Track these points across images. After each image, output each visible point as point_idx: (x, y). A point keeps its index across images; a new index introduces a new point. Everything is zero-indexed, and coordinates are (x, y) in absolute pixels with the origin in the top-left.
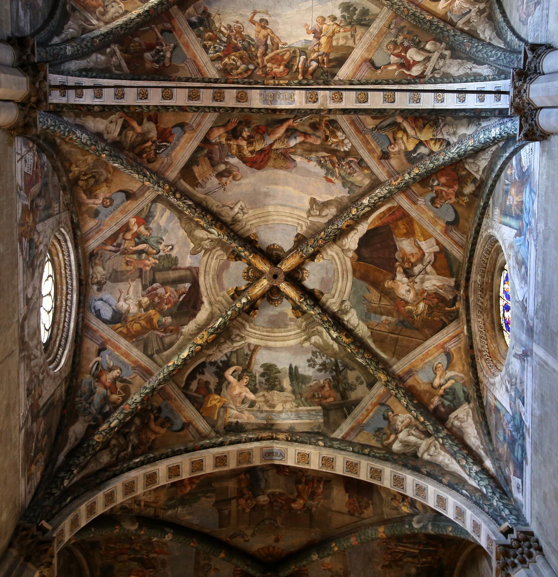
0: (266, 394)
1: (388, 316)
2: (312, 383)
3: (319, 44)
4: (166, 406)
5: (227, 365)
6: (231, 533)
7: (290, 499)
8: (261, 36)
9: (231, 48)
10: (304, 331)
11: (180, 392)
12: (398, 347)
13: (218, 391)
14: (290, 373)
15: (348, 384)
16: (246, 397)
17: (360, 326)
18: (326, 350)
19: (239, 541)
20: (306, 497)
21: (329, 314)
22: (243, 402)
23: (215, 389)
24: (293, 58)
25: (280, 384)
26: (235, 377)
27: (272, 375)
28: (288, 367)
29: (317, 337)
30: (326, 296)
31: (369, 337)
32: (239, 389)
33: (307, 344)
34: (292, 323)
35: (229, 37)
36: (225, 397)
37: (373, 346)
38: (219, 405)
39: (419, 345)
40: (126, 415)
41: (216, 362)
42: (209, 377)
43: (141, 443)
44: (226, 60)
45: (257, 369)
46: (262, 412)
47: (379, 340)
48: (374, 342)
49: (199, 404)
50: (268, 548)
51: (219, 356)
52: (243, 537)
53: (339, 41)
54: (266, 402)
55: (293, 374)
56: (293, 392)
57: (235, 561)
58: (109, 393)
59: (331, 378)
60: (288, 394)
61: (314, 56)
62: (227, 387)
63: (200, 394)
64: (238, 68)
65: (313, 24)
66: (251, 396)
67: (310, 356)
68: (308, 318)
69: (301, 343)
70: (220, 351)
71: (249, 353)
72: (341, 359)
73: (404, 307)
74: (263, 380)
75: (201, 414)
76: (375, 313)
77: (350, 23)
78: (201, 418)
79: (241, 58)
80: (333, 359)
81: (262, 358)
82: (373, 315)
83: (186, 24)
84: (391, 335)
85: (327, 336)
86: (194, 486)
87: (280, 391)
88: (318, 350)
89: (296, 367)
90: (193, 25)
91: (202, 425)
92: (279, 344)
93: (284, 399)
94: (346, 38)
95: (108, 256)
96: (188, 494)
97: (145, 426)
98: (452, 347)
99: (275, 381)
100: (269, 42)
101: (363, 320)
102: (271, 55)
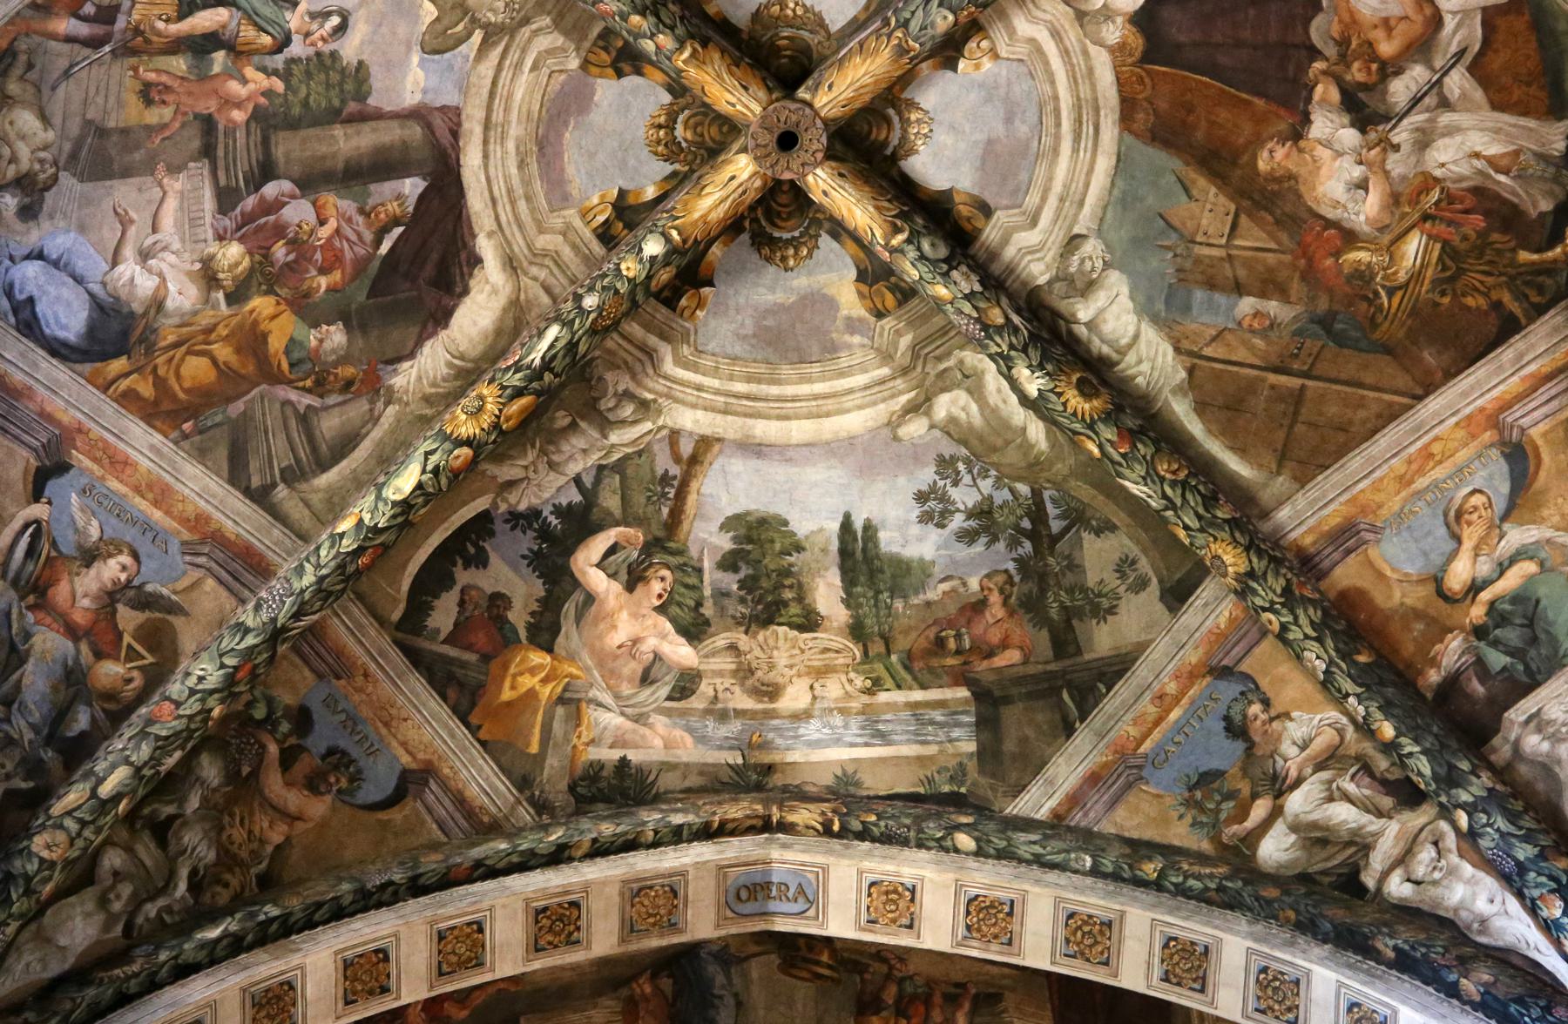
0: (743, 641)
1: (1263, 295)
5: (581, 521)
10: (905, 371)
12: (1300, 429)
13: (544, 633)
14: (845, 553)
16: (657, 657)
17: (1142, 344)
18: (995, 450)
21: (1010, 297)
22: (646, 679)
23: (531, 628)
25: (800, 599)
26: (613, 576)
27: (770, 563)
28: (834, 526)
29: (961, 396)
30: (1001, 218)
31: (1179, 390)
32: (629, 620)
33: (916, 428)
34: (856, 339)
36: (572, 658)
37: (1195, 427)
38: (546, 692)
39: (1391, 415)
40: (164, 745)
41: (535, 513)
42: (508, 577)
43: (228, 859)
46: (723, 716)
47: (1223, 399)
48: (1201, 408)
49: (464, 693)
51: (547, 487)
54: (744, 673)
55: (858, 555)
56: (857, 631)
60: (832, 638)
62: (579, 619)
66: (681, 652)
67: (927, 475)
68: (925, 318)
69: (893, 424)
70: (552, 466)
71: (675, 470)
72: (1057, 486)
73: (1337, 254)
74: (731, 582)
75: (474, 730)
76: (1211, 285)
78: (476, 751)
80: (1023, 489)
81: (725, 493)
82: (1199, 295)
84: (1273, 378)
85: (1002, 393)
87: (802, 628)
88: (964, 451)
89: (869, 527)
91: (481, 780)
92: (799, 430)
95: (63, 63)
97: (243, 786)
98: (1535, 422)
99: (779, 586)
101: (1155, 320)
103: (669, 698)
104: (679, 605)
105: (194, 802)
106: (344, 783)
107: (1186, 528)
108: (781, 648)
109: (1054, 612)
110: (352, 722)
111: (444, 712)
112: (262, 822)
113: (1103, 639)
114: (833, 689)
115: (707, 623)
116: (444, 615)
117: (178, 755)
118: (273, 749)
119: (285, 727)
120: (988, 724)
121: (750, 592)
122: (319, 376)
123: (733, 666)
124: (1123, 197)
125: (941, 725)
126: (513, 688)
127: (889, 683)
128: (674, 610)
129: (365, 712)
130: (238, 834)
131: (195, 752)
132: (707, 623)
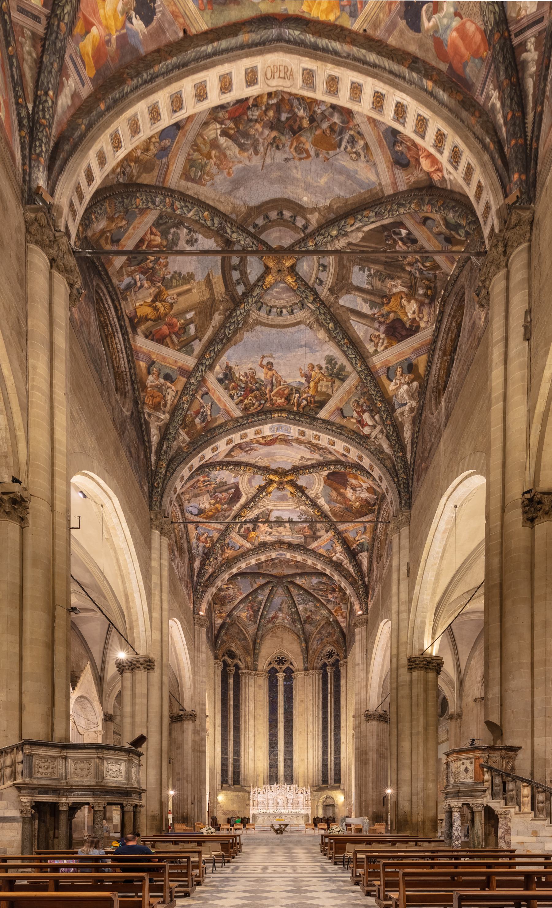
3: (309, 387)
8: (268, 377)
9: (248, 391)
24: (291, 394)
35: (246, 383)
44: (246, 401)
53: (323, 387)
61: (305, 396)
64: (254, 404)
65: (305, 369)
77: (331, 375)
79: (255, 397)
83: (216, 382)
90: (220, 381)
94: (327, 386)
100: (274, 381)
102: (275, 390)
108: (281, 529)
113: (318, 534)
116: (242, 530)
122: (225, 510)
124: (324, 490)
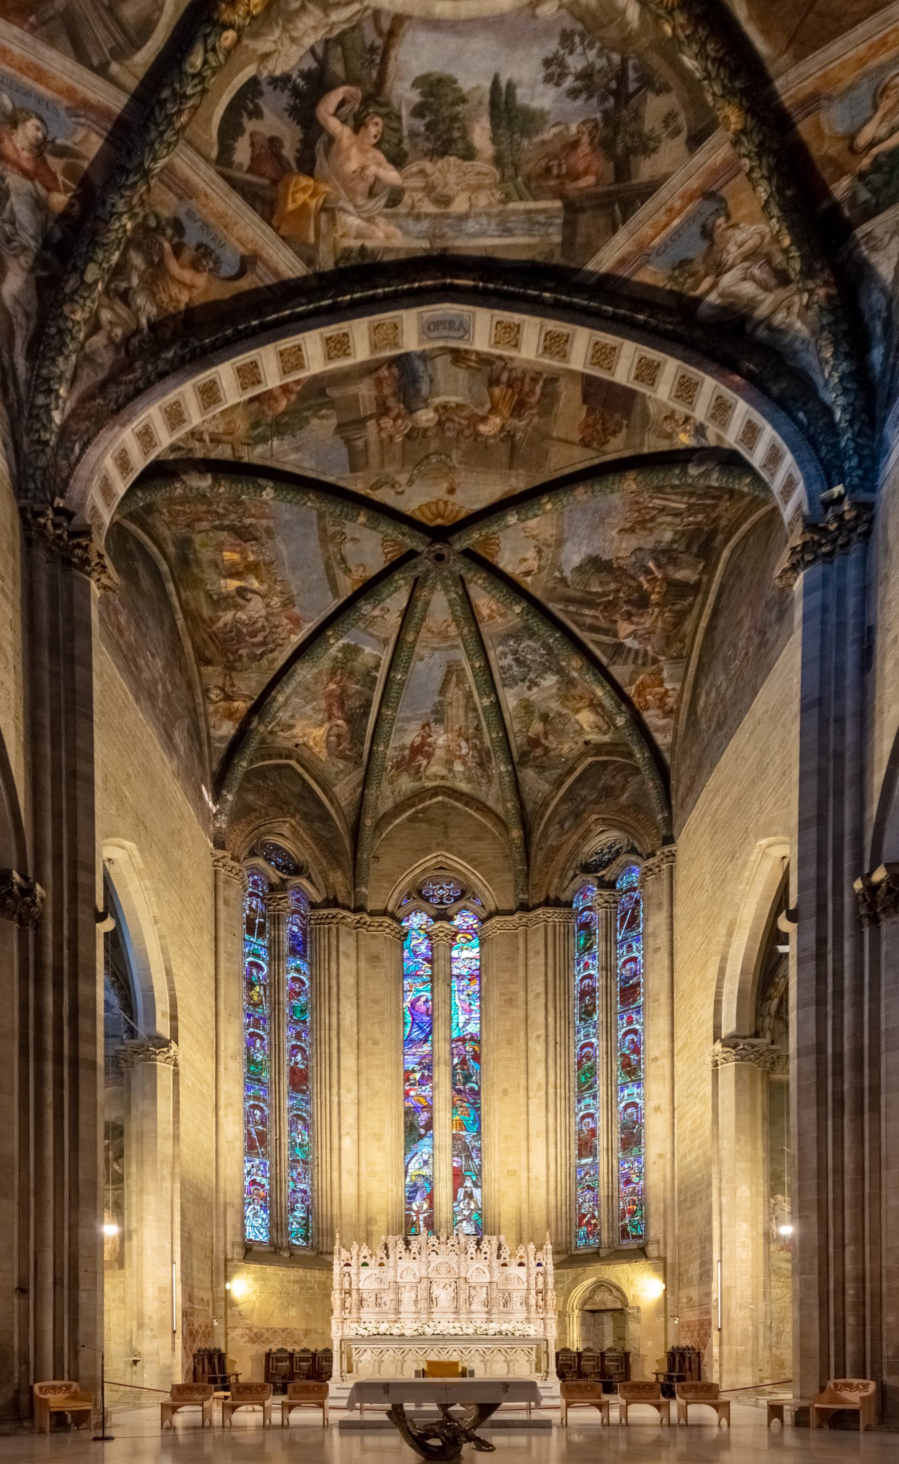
0: (429, 167)
2: (548, 134)
4: (190, 214)
6: (373, 481)
7: (476, 415)
11: (211, 173)
15: (641, 135)
16: (377, 179)
19: (384, 496)
20: (506, 412)
38: (313, 203)
45: (404, 93)
46: (418, 217)
50: (437, 503)
52: (393, 487)
54: (429, 189)
57: (383, 528)
58: (42, 192)
59: (598, 116)
60: (483, 165)
62: (327, 152)
63: (262, 175)
66: (391, 175)
74: (420, 125)
81: (416, 58)
86: (293, 397)
93: (473, 180)
96: (284, 413)
99: (450, 129)
103: (386, 206)
104: (388, 142)
105: (135, 281)
106: (211, 264)
107: (714, 94)
108: (448, 172)
109: (619, 150)
110: (206, 226)
111: (256, 218)
112: (175, 290)
114: (482, 200)
115: (406, 155)
117: (117, 254)
118: (167, 245)
119: (169, 232)
120: (569, 225)
121: (433, 132)
123: (422, 184)
125: (543, 225)
126: (294, 201)
127: (515, 197)
128: (385, 146)
129: (212, 220)
130: (165, 298)
131: (126, 249)
132: (406, 155)
